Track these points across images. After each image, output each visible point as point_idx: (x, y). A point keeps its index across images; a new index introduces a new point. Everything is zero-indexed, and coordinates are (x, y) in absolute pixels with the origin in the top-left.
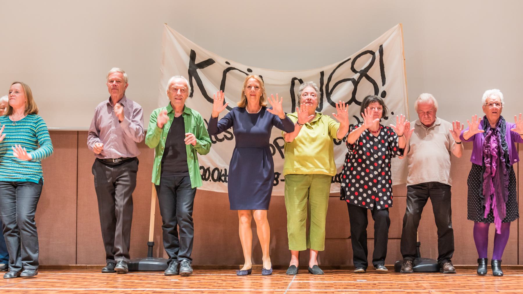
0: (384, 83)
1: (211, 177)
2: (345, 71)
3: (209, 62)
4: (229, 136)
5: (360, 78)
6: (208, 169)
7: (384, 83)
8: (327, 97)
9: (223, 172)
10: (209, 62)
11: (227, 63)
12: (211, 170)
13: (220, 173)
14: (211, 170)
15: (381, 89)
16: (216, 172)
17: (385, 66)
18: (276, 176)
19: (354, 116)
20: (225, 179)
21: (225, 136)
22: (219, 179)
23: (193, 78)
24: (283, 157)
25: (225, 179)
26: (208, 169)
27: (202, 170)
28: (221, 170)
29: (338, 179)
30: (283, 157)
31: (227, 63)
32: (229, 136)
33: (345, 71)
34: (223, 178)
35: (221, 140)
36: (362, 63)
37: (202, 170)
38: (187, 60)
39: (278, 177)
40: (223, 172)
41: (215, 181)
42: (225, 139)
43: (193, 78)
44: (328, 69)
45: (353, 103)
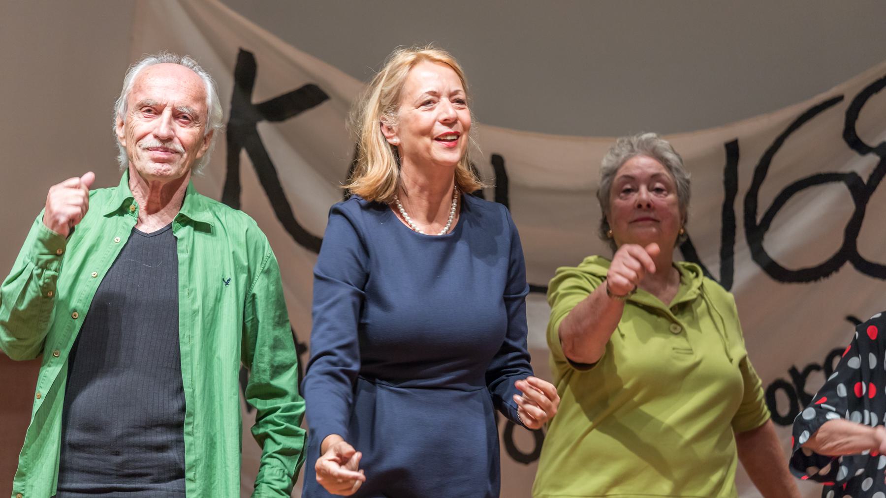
23: (244, 155)
43: (244, 155)
44: (754, 130)
45: (848, 266)
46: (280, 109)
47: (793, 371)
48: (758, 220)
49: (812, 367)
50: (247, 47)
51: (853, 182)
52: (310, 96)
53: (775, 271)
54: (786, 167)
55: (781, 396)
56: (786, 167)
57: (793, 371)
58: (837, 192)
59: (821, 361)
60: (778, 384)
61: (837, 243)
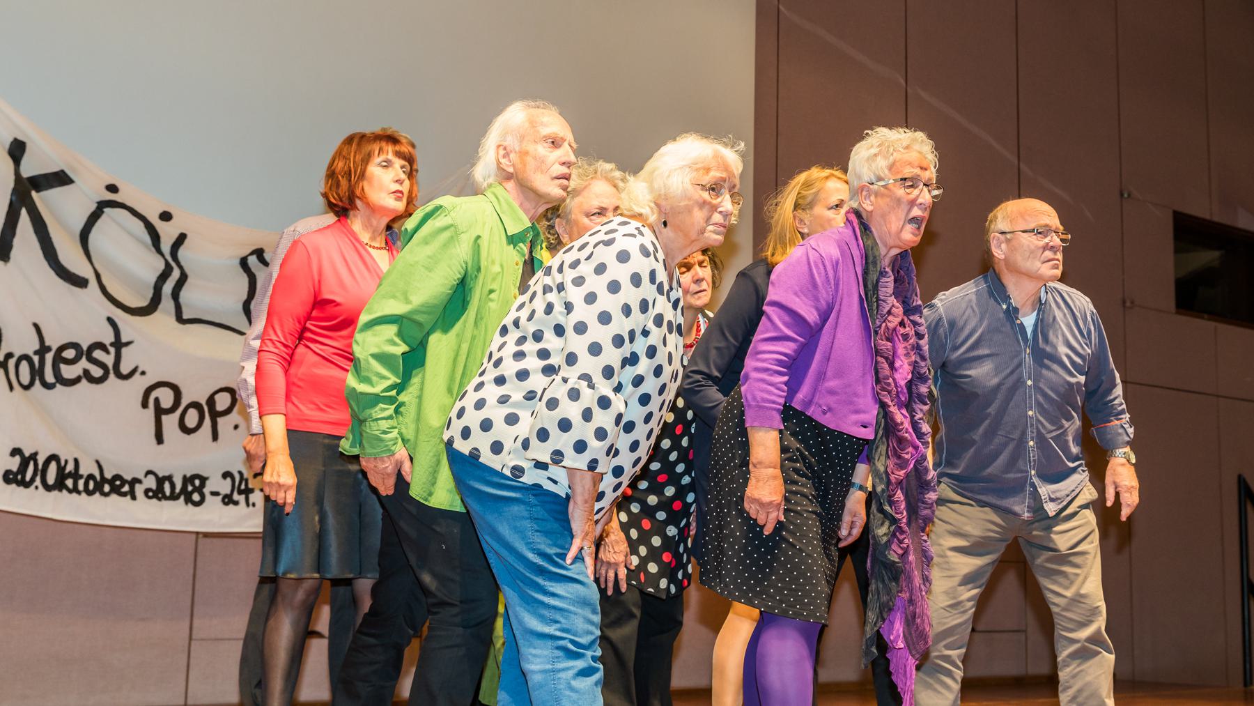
1: (38, 479)
4: (97, 372)
6: (34, 456)
9: (70, 467)
12: (41, 460)
13: (61, 469)
14: (41, 460)
16: (53, 467)
18: (197, 482)
20: (75, 484)
22: (60, 485)
24: (215, 437)
25: (75, 484)
26: (34, 456)
27: (17, 459)
28: (66, 462)
30: (215, 437)
32: (97, 372)
34: (69, 483)
37: (17, 459)
39: (203, 484)
40: (70, 467)
41: (48, 488)
50: (20, 138)
52: (61, 179)
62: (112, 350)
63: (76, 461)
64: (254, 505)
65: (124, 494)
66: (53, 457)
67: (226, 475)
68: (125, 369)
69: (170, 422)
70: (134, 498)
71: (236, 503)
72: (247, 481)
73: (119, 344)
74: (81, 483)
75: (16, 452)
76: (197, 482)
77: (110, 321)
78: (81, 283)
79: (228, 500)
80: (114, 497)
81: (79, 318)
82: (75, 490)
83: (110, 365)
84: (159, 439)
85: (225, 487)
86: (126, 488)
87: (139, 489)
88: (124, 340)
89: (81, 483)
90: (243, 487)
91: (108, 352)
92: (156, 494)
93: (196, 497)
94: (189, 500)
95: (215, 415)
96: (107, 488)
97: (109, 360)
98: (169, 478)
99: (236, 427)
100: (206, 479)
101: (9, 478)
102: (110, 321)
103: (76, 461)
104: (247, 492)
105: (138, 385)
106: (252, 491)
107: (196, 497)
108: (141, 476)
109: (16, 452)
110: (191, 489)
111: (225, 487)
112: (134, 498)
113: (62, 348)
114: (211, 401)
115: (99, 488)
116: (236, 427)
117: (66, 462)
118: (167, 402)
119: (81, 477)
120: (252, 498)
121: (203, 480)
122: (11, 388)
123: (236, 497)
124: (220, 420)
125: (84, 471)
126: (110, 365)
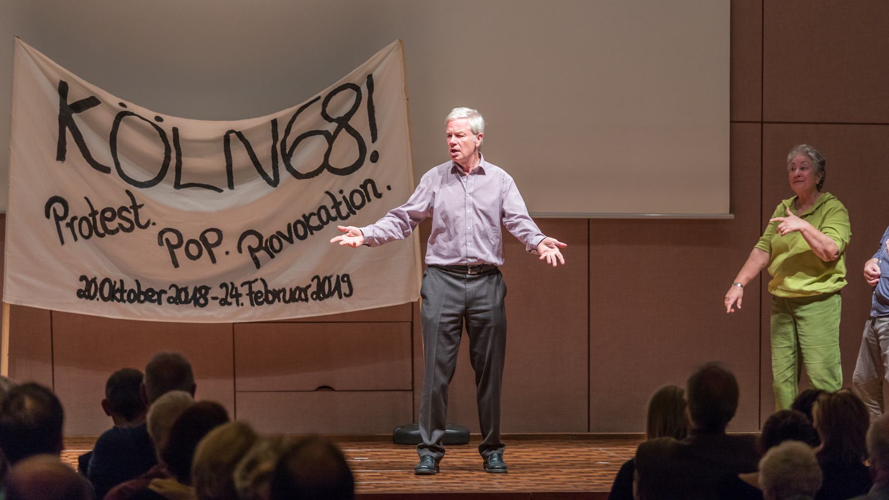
0: (374, 139)
1: (98, 294)
2: (311, 119)
3: (93, 101)
4: (127, 225)
5: (337, 132)
7: (374, 139)
8: (285, 162)
9: (118, 286)
10: (93, 101)
11: (122, 104)
12: (99, 282)
13: (112, 287)
14: (99, 282)
15: (371, 148)
16: (107, 285)
17: (376, 109)
18: (203, 291)
19: (327, 193)
20: (122, 296)
21: (120, 225)
22: (112, 297)
23: (67, 128)
24: (214, 261)
25: (122, 296)
27: (84, 282)
28: (115, 282)
29: (303, 296)
30: (214, 261)
31: (122, 104)
32: (127, 225)
33: (311, 119)
34: (118, 295)
35: (113, 232)
36: (342, 105)
37: (84, 282)
38: (55, 98)
39: (207, 293)
40: (118, 286)
41: (105, 299)
42: (121, 231)
43: (67, 128)
44: (283, 115)
46: (80, 106)
47: (304, 216)
48: (287, 151)
49: (312, 214)
51: (326, 134)
53: (297, 175)
54: (299, 128)
55: (299, 226)
56: (299, 128)
57: (304, 216)
58: (320, 140)
59: (316, 212)
60: (298, 222)
61: (321, 161)
62: (132, 211)
63: (122, 281)
64: (242, 305)
65: (154, 301)
66: (107, 280)
67: (223, 285)
68: (143, 222)
69: (180, 253)
70: (160, 303)
71: (230, 304)
72: (236, 289)
73: (136, 207)
74: (125, 295)
75: (83, 278)
76: (203, 291)
77: (128, 192)
78: (107, 170)
79: (224, 302)
80: (147, 304)
81: (109, 193)
82: (122, 300)
83: (133, 219)
84: (176, 265)
85: (221, 294)
86: (155, 297)
87: (164, 297)
88: (138, 204)
89: (125, 295)
90: (234, 293)
91: (130, 213)
92: (176, 300)
93: (202, 301)
94: (197, 303)
95: (209, 247)
96: (142, 298)
97: (132, 217)
98: (185, 290)
99: (227, 253)
100: (210, 288)
101: (81, 294)
102: (128, 192)
103: (122, 281)
104: (238, 296)
105: (153, 231)
106: (241, 295)
107: (202, 301)
108: (167, 289)
109: (83, 278)
110: (199, 296)
111: (221, 294)
112: (160, 303)
113: (104, 211)
114: (203, 236)
115: (137, 298)
116: (227, 253)
117: (115, 282)
118: (174, 240)
119: (126, 291)
120: (241, 300)
121: (207, 289)
122: (76, 239)
123: (229, 300)
124: (214, 250)
125: (127, 287)
126: (133, 219)
